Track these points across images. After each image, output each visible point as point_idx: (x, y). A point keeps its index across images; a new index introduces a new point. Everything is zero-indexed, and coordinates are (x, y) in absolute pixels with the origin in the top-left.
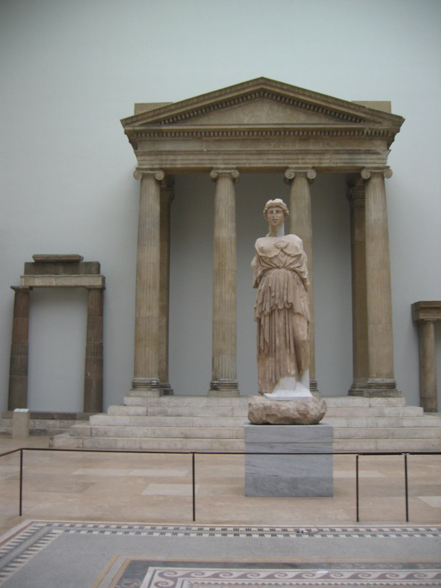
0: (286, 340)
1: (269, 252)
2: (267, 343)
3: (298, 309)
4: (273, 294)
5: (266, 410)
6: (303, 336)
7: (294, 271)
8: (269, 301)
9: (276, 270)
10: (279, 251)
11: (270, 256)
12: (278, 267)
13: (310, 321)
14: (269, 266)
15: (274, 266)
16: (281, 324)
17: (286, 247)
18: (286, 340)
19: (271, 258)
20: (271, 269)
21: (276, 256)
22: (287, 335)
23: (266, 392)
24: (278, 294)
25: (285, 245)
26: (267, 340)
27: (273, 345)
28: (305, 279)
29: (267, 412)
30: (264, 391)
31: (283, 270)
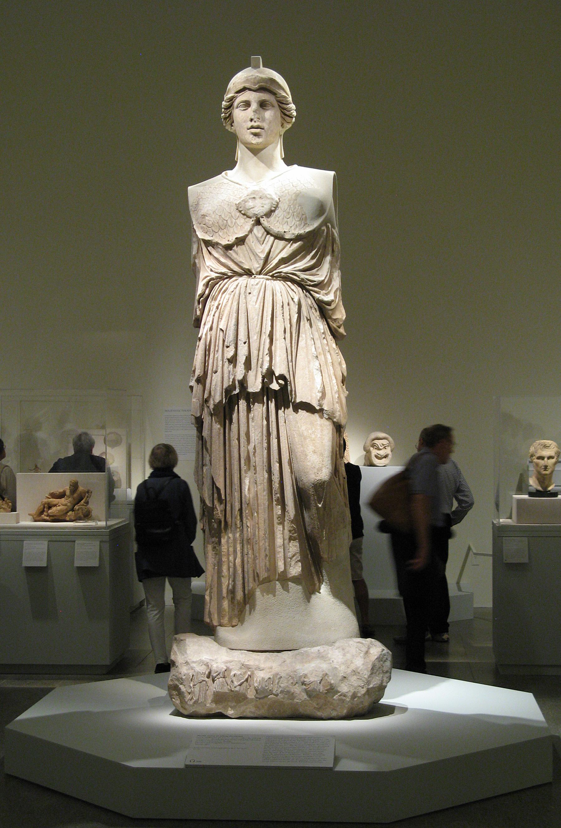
0: (270, 480)
1: (220, 228)
2: (218, 490)
3: (302, 393)
4: (230, 353)
5: (214, 681)
6: (320, 469)
7: (293, 281)
8: (220, 370)
9: (243, 280)
10: (251, 222)
11: (224, 242)
12: (249, 273)
13: (343, 422)
14: (224, 270)
15: (236, 269)
16: (256, 435)
17: (269, 214)
18: (270, 480)
19: (228, 247)
20: (230, 277)
21: (241, 241)
22: (276, 467)
23: (221, 625)
24: (243, 351)
25: (266, 209)
26: (220, 484)
27: (237, 495)
28: (329, 303)
29: (215, 687)
30: (215, 623)
31: (260, 280)
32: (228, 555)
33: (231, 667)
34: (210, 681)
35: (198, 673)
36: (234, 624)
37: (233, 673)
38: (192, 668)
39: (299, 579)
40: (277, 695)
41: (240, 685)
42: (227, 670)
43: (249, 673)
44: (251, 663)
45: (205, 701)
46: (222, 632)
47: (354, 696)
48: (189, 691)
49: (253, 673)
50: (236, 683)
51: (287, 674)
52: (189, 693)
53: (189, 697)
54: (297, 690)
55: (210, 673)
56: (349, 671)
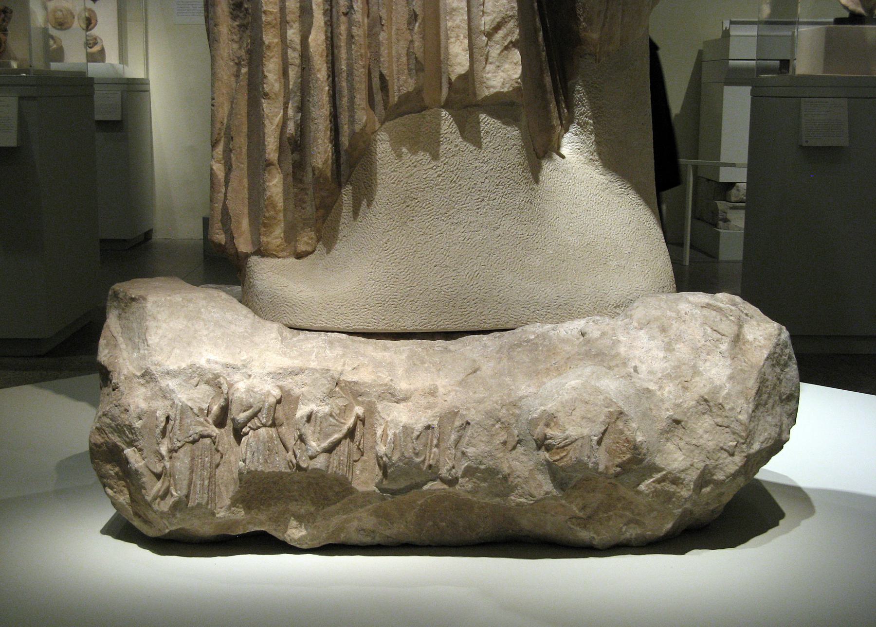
5: (238, 435)
23: (262, 252)
29: (243, 456)
30: (243, 245)
32: (284, 23)
33: (297, 391)
34: (225, 435)
35: (185, 410)
36: (302, 248)
37: (302, 411)
38: (165, 394)
39: (512, 104)
40: (452, 482)
41: (330, 450)
42: (285, 400)
43: (359, 410)
44: (364, 376)
45: (211, 500)
46: (267, 274)
47: (704, 479)
48: (158, 469)
49: (371, 410)
50: (314, 445)
51: (489, 414)
52: (158, 476)
53: (158, 487)
54: (521, 464)
55: (225, 410)
56: (689, 400)
